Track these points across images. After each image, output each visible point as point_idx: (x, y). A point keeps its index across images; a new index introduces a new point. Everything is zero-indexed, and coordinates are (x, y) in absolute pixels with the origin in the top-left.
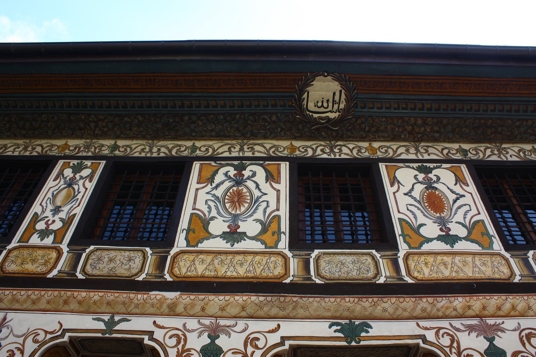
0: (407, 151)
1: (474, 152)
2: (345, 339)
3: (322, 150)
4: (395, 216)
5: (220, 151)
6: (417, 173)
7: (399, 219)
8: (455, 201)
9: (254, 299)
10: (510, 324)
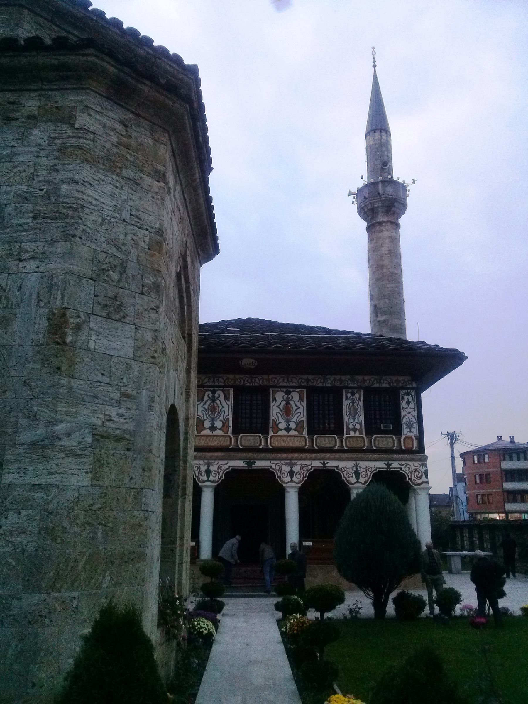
0: (283, 380)
1: (312, 381)
2: (247, 467)
3: (247, 381)
4: (271, 418)
5: (205, 381)
6: (284, 394)
7: (273, 420)
8: (295, 411)
9: (220, 454)
10: (299, 462)
